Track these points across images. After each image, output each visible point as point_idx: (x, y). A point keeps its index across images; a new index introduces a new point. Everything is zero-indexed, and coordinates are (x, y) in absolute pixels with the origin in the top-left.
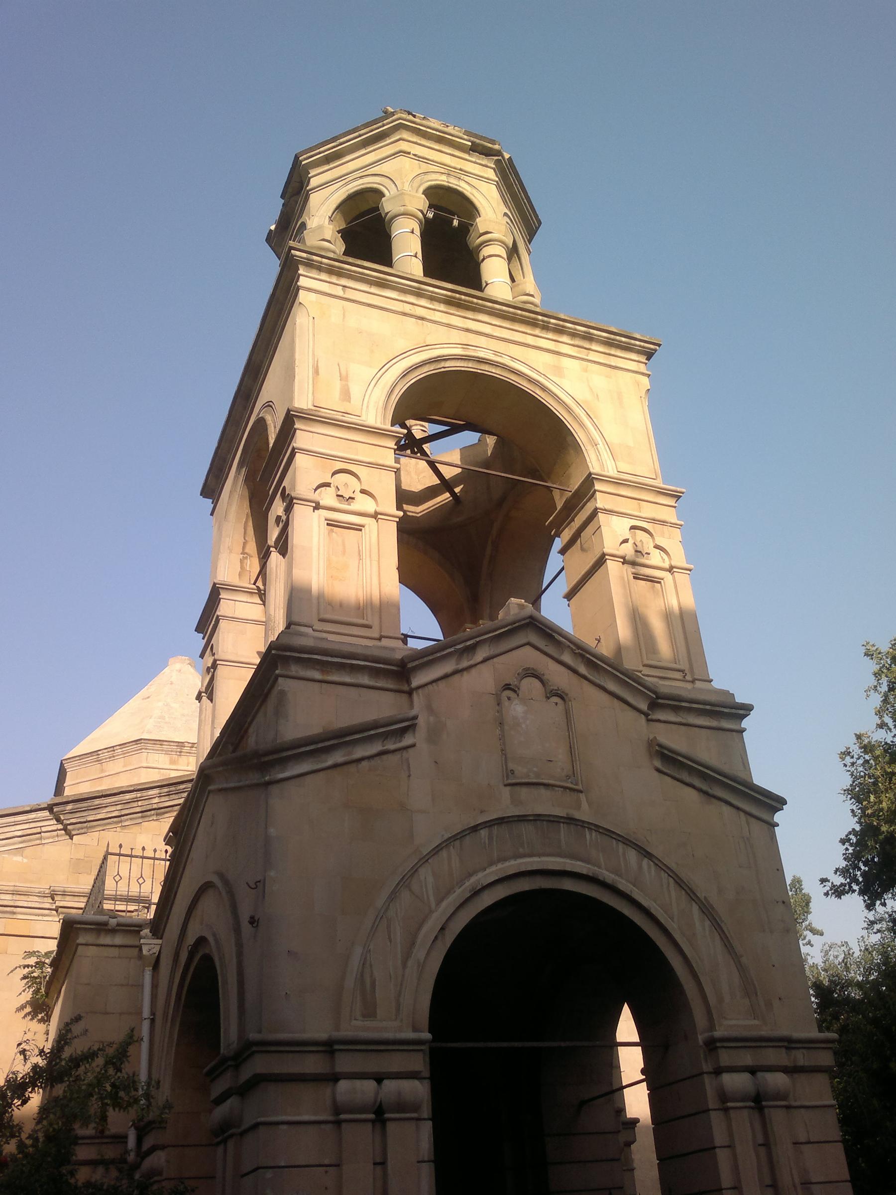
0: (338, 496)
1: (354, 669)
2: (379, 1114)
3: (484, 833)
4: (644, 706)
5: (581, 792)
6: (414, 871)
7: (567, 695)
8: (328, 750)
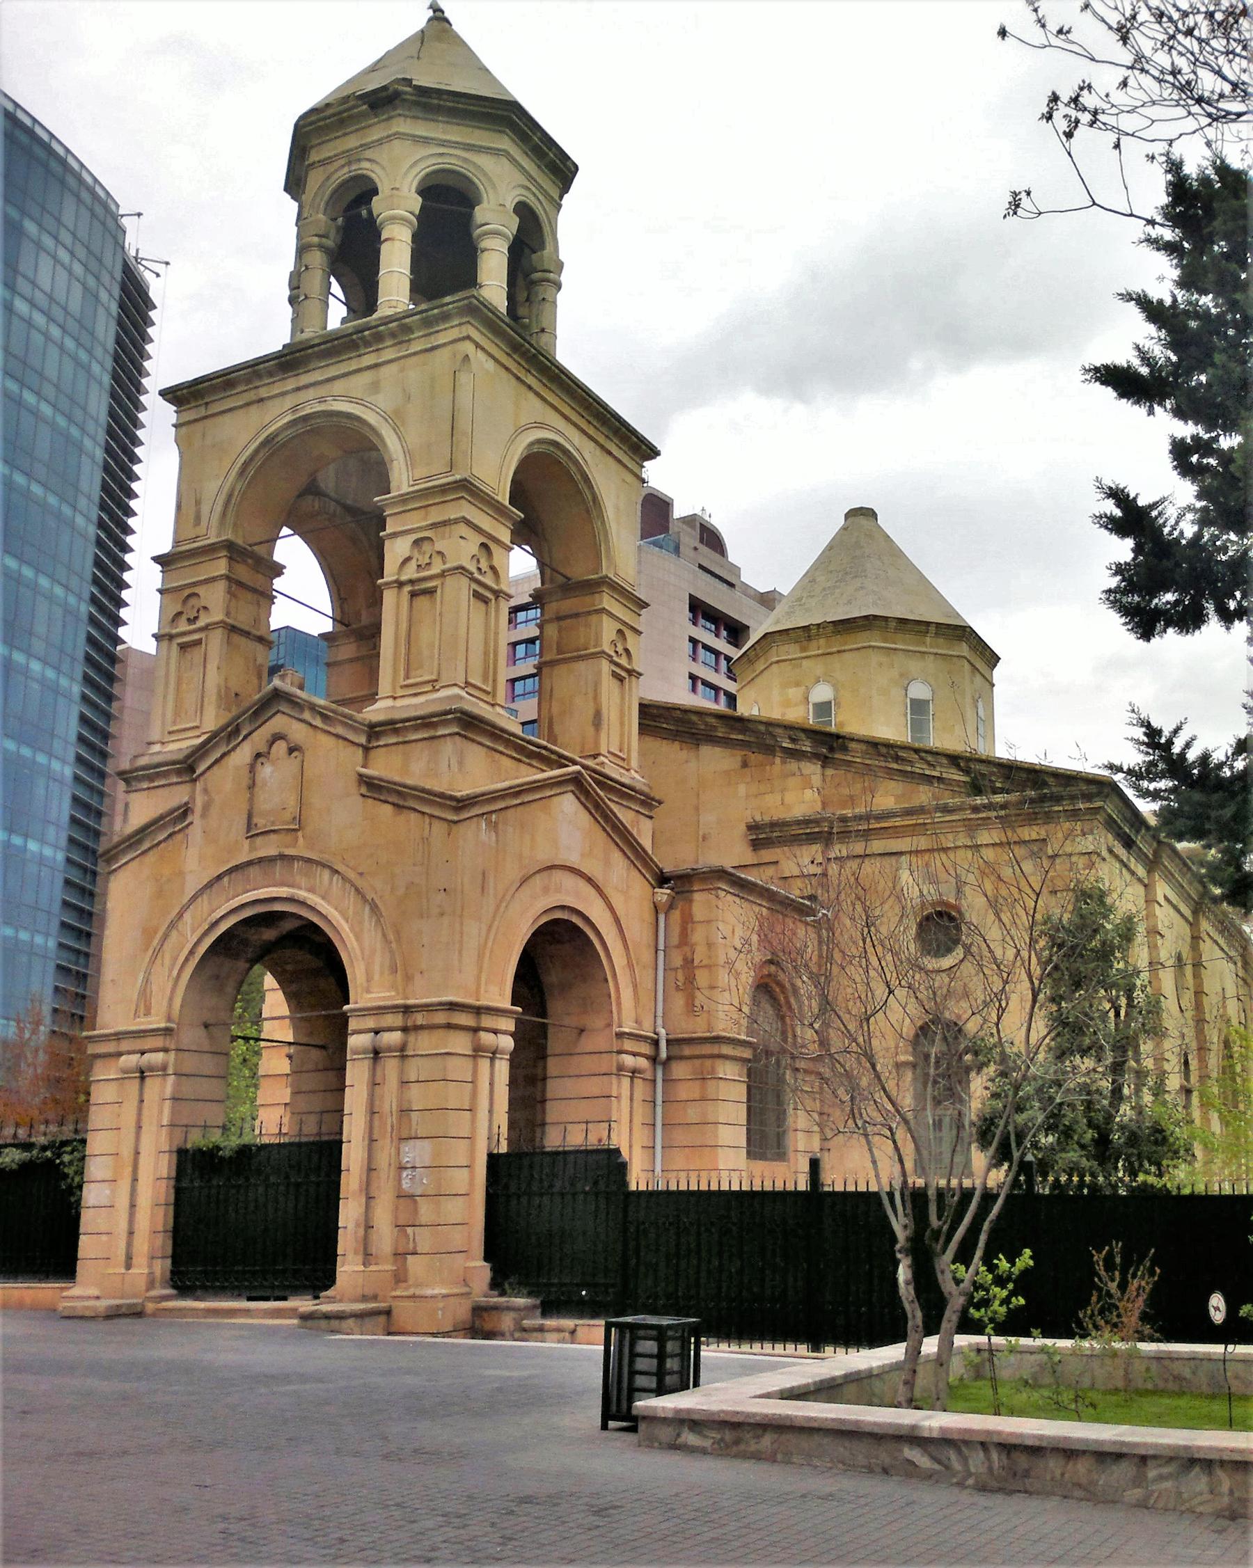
2: (142, 1074)
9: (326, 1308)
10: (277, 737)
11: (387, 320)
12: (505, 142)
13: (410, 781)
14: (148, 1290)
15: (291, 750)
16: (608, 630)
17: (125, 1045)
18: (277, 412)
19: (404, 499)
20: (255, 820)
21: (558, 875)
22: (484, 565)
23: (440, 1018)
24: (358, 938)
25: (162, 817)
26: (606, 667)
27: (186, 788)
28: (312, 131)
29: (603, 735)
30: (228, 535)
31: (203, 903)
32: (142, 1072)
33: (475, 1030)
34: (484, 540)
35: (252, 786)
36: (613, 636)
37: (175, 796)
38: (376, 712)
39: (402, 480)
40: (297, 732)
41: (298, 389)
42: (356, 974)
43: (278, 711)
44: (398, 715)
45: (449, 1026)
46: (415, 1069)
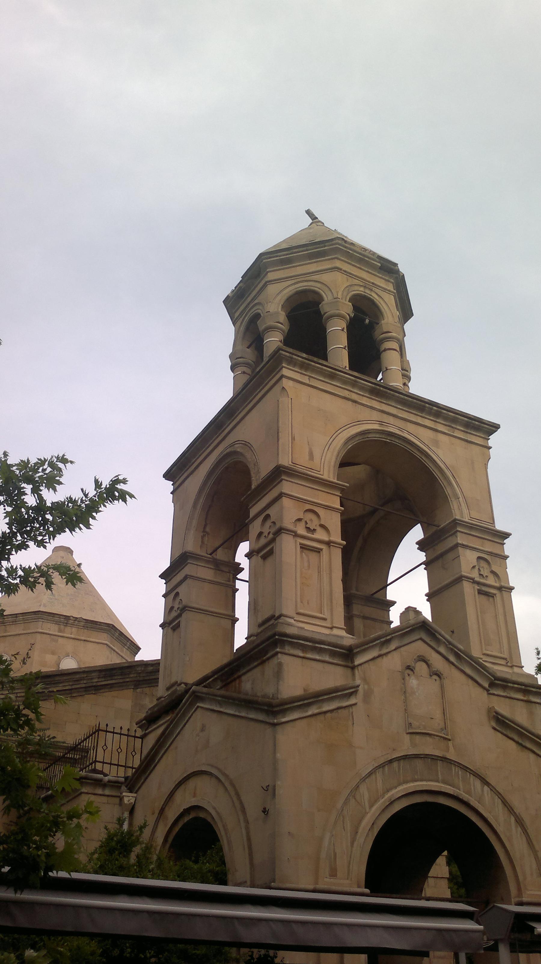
0: (307, 528)
1: (320, 651)
3: (395, 764)
4: (486, 685)
5: (450, 740)
6: (357, 787)
7: (442, 675)
8: (309, 705)
37: (332, 676)
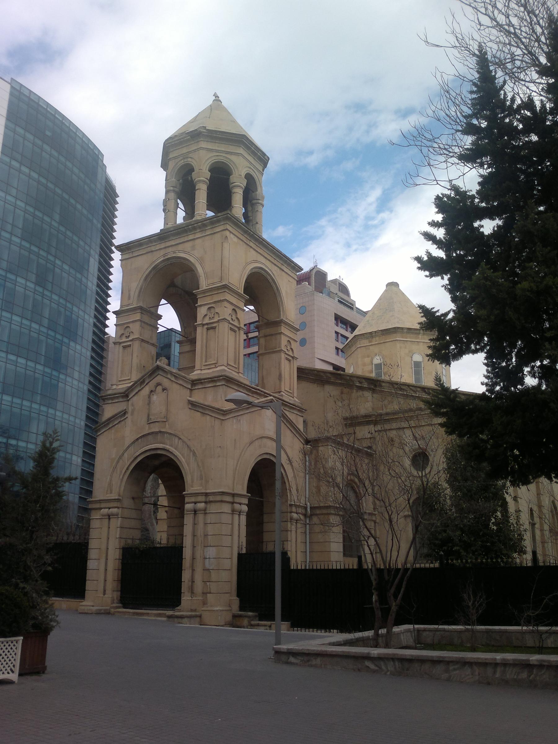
1: (118, 397)
2: (109, 517)
6: (123, 454)
9: (177, 614)
10: (158, 384)
11: (198, 222)
12: (241, 151)
13: (206, 403)
14: (112, 604)
15: (164, 390)
16: (284, 341)
17: (103, 505)
18: (158, 257)
19: (204, 292)
20: (151, 417)
21: (265, 440)
22: (234, 317)
23: (219, 498)
24: (188, 464)
25: (116, 415)
26: (283, 356)
27: (125, 403)
28: (170, 146)
29: (283, 383)
30: (141, 304)
31: (132, 449)
32: (109, 516)
33: (233, 503)
34: (234, 307)
35: (149, 404)
36: (286, 343)
38: (195, 375)
39: (204, 284)
40: (166, 383)
41: (165, 248)
42: (188, 479)
43: (159, 374)
44: (202, 377)
45: (222, 501)
46: (210, 518)
